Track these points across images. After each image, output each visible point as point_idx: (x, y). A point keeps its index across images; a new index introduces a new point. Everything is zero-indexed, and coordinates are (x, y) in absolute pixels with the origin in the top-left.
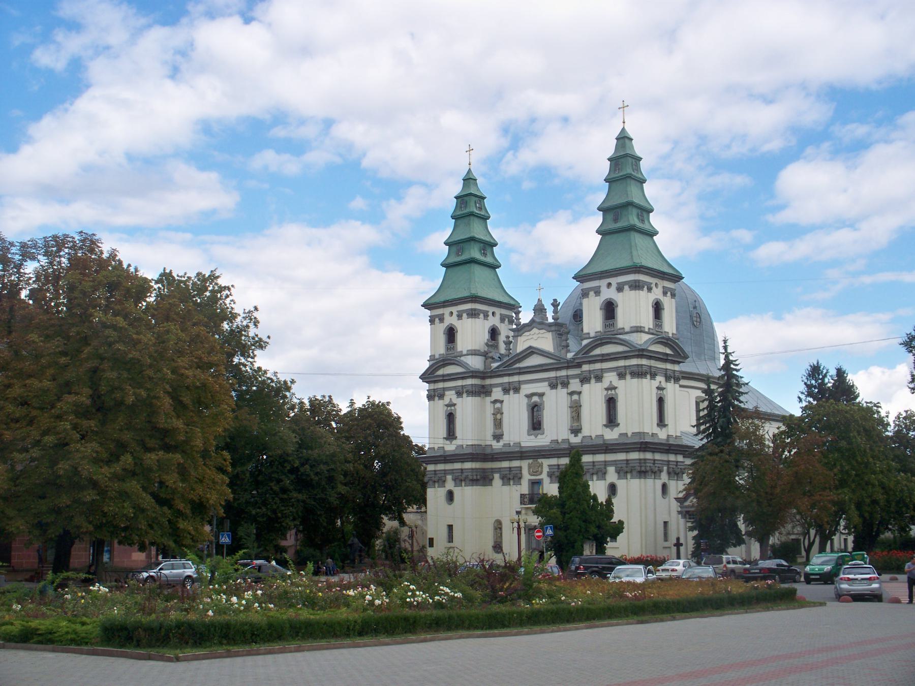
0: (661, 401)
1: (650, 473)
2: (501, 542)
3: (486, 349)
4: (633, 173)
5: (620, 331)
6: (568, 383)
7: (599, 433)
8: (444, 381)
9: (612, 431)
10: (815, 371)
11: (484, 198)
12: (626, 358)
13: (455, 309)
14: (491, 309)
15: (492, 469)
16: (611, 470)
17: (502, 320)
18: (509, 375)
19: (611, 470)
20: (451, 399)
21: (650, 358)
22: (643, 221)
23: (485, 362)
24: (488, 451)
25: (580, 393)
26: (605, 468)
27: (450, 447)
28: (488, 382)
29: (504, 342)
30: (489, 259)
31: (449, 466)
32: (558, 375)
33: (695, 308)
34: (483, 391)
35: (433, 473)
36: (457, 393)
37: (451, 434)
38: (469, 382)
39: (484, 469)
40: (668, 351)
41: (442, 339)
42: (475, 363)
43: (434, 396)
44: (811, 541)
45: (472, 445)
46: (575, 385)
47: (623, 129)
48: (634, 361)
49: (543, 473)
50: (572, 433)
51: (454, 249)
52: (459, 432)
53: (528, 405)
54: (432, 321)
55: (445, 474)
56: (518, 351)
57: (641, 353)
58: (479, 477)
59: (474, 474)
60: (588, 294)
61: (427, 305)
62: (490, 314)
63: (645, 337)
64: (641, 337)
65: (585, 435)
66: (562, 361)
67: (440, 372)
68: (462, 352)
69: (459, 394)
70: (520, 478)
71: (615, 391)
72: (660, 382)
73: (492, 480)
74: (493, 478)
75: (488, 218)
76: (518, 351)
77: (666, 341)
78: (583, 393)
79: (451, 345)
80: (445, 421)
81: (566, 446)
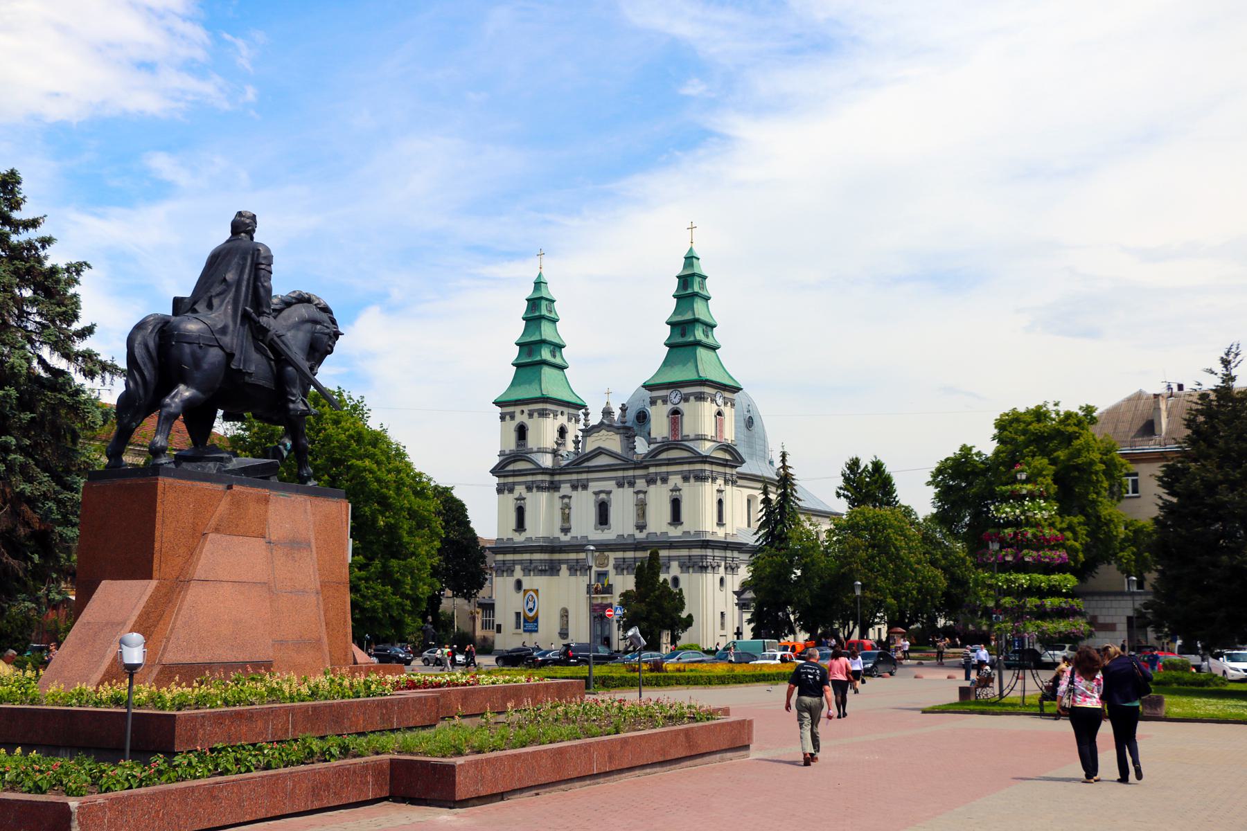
0: (720, 502)
1: (710, 568)
2: (567, 629)
3: (555, 447)
4: (700, 291)
5: (685, 438)
6: (635, 483)
8: (514, 476)
10: (854, 464)
11: (553, 301)
12: (690, 463)
13: (526, 408)
14: (560, 409)
15: (559, 560)
16: (674, 564)
17: (570, 420)
18: (578, 473)
19: (674, 564)
21: (712, 463)
22: (707, 336)
23: (554, 460)
24: (556, 544)
25: (645, 492)
27: (519, 538)
28: (557, 478)
30: (558, 361)
31: (518, 557)
33: (749, 411)
34: (554, 487)
37: (520, 526)
38: (539, 478)
39: (551, 560)
40: (728, 457)
41: (513, 436)
42: (547, 461)
44: (851, 630)
46: (641, 484)
47: (691, 249)
48: (698, 467)
51: (526, 349)
53: (596, 502)
54: (503, 418)
62: (559, 413)
63: (708, 445)
65: (651, 531)
67: (510, 468)
69: (529, 489)
73: (559, 570)
75: (558, 320)
77: (727, 448)
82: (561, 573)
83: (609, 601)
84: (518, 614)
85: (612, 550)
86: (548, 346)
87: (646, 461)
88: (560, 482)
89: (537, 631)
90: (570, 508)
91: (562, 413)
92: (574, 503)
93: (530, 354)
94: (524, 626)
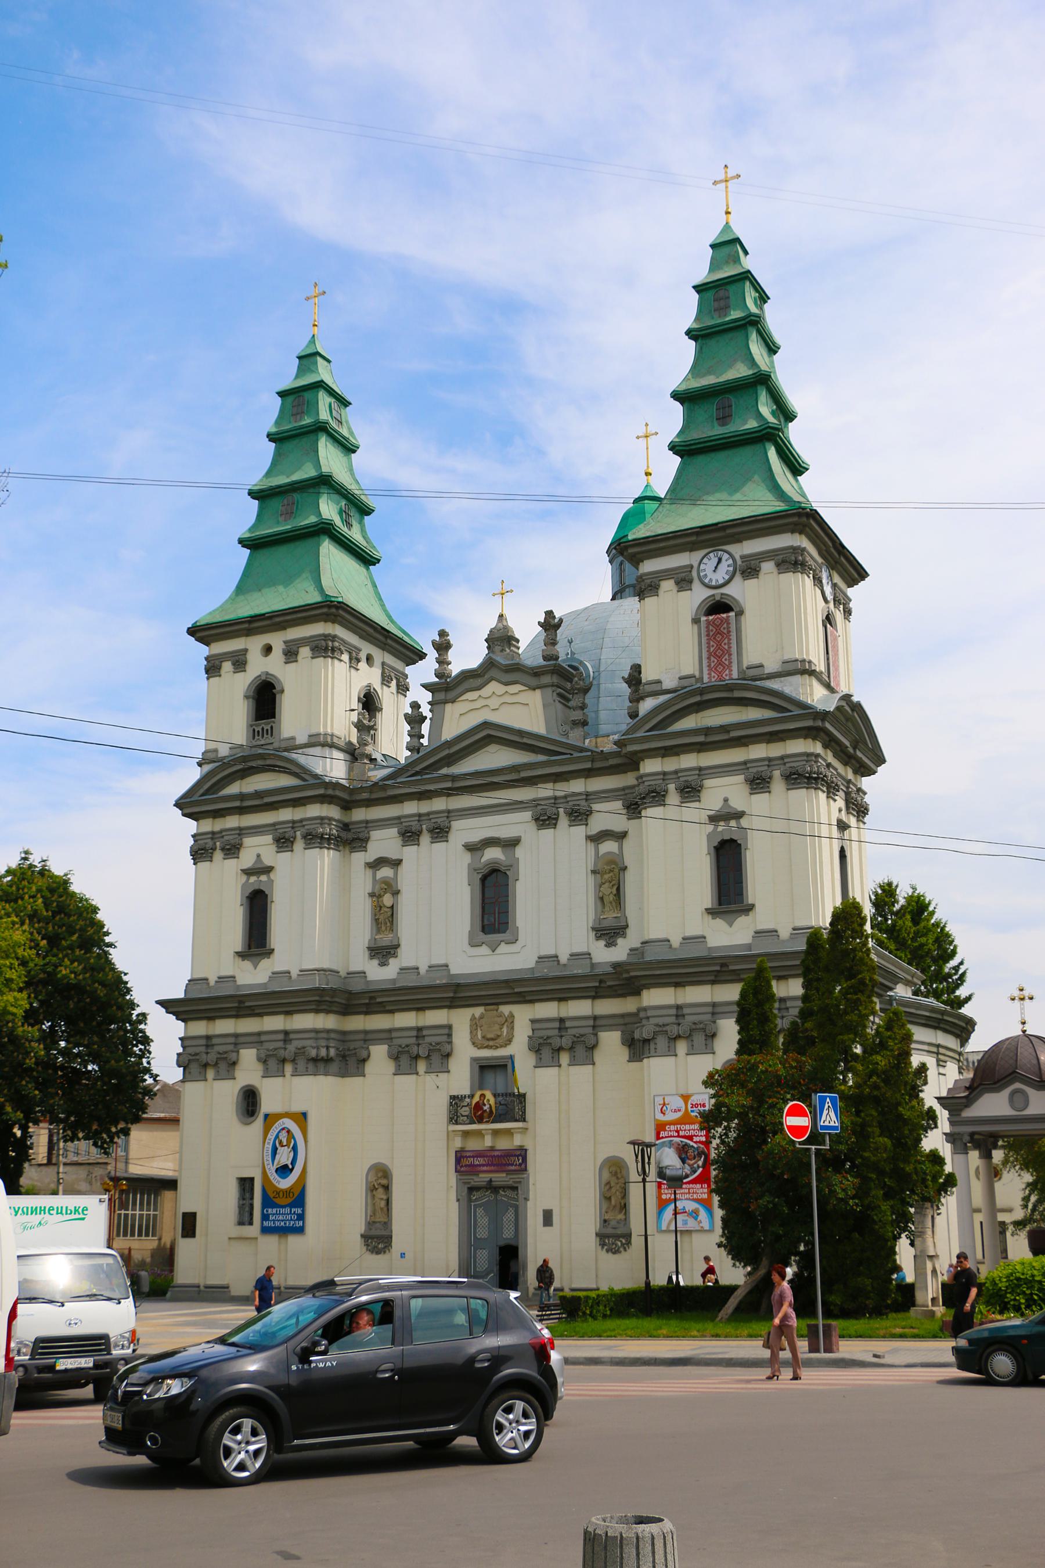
2: (387, 1224)
7: (693, 929)
8: (241, 811)
9: (731, 925)
13: (277, 640)
14: (366, 648)
17: (386, 680)
20: (258, 856)
23: (350, 770)
24: (357, 986)
25: (621, 836)
26: (714, 1022)
28: (359, 814)
29: (406, 716)
35: (203, 1042)
38: (314, 811)
39: (344, 1033)
43: (214, 849)
47: (727, 227)
48: (797, 746)
49: (514, 1040)
50: (598, 938)
53: (472, 869)
54: (212, 668)
56: (443, 739)
57: (819, 723)
58: (332, 1052)
59: (323, 1043)
60: (659, 586)
61: (200, 632)
62: (363, 656)
65: (653, 935)
66: (576, 754)
67: (234, 789)
68: (293, 738)
69: (284, 842)
70: (448, 1055)
71: (738, 823)
72: (840, 810)
74: (369, 1056)
76: (448, 733)
78: (629, 832)
79: (265, 724)
81: (580, 969)
82: (369, 1067)
83: (517, 1141)
84: (246, 1184)
85: (524, 999)
86: (336, 497)
88: (369, 825)
89: (301, 1230)
90: (396, 893)
91: (369, 659)
92: (407, 878)
93: (289, 514)
94: (265, 1217)
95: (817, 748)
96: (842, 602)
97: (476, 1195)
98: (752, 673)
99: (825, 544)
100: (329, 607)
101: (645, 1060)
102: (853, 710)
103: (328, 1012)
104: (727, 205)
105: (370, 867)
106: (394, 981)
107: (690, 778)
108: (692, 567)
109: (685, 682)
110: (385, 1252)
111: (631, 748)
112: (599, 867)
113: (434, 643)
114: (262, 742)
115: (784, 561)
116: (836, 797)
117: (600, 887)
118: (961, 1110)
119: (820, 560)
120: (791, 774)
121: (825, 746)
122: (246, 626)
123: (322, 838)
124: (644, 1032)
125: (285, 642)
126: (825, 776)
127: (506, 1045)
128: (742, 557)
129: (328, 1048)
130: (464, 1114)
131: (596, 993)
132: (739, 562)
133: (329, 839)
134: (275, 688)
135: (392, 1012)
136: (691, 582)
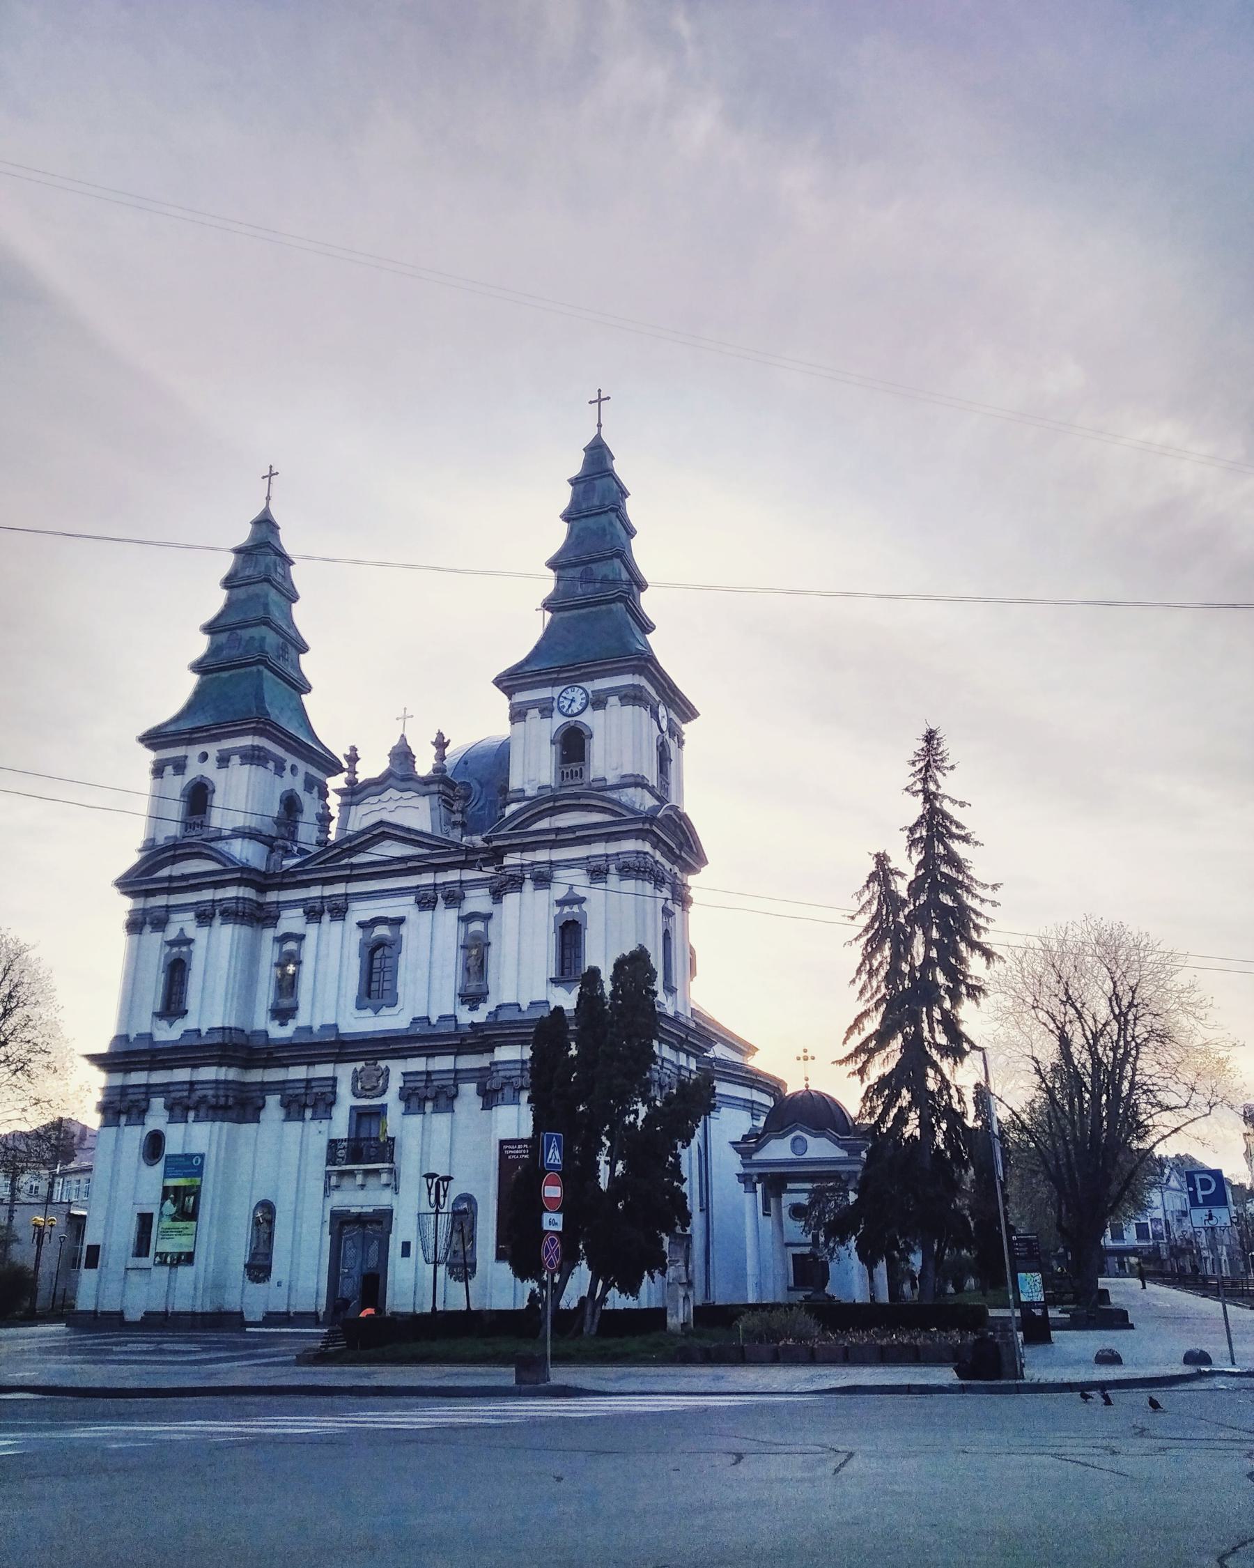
2: (268, 1256)
8: (170, 891)
13: (213, 749)
14: (290, 760)
15: (262, 1083)
20: (182, 930)
23: (268, 859)
24: (259, 1043)
27: (168, 1033)
28: (272, 896)
31: (159, 1077)
32: (439, 881)
36: (198, 916)
37: (173, 1006)
38: (231, 892)
45: (223, 1028)
46: (478, 901)
48: (630, 845)
50: (463, 1003)
52: (193, 1000)
53: (363, 944)
54: (158, 771)
55: (146, 1093)
57: (647, 826)
59: (221, 1092)
62: (288, 766)
64: (643, 797)
69: (204, 917)
70: (333, 1103)
71: (580, 908)
74: (264, 1106)
80: (162, 977)
81: (448, 1028)
84: (145, 1221)
87: (499, 838)
90: (298, 963)
95: (647, 847)
96: (674, 732)
97: (347, 1229)
98: (595, 785)
99: (662, 685)
100: (257, 722)
101: (494, 1108)
102: (680, 820)
103: (230, 1066)
104: (599, 419)
105: (278, 941)
106: (290, 1039)
107: (542, 870)
108: (553, 699)
109: (543, 791)
110: (264, 1281)
111: (495, 844)
112: (469, 942)
113: (346, 756)
114: (194, 834)
115: (625, 696)
116: (662, 889)
117: (467, 960)
118: (752, 1154)
119: (658, 699)
120: (624, 868)
121: (655, 847)
122: (187, 736)
123: (237, 915)
124: (492, 1084)
125: (218, 751)
126: (652, 870)
127: (380, 1095)
128: (592, 692)
129: (227, 1097)
130: (340, 1155)
131: (459, 1049)
132: (591, 696)
133: (244, 915)
134: (206, 787)
135: (287, 1066)
136: (552, 710)
